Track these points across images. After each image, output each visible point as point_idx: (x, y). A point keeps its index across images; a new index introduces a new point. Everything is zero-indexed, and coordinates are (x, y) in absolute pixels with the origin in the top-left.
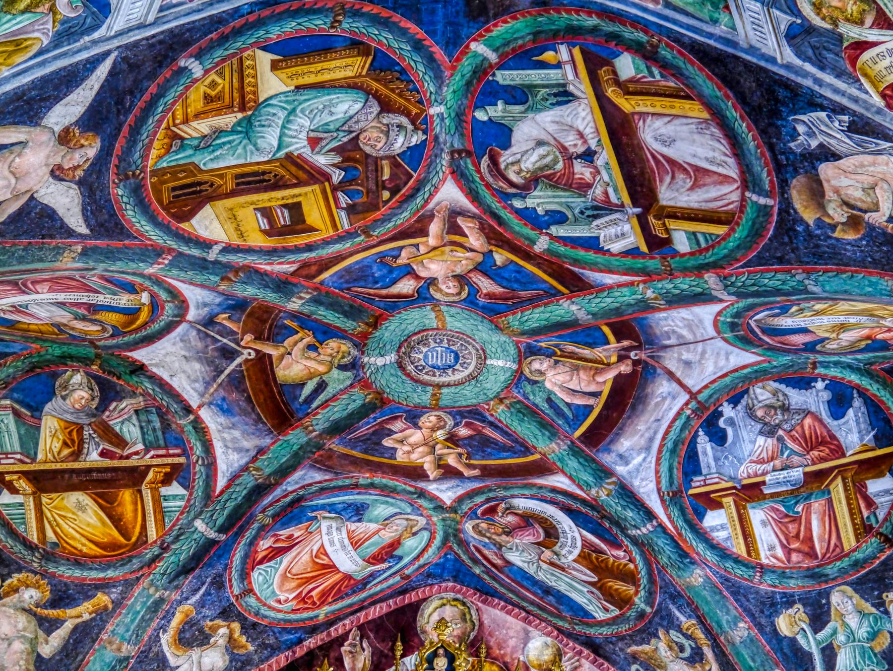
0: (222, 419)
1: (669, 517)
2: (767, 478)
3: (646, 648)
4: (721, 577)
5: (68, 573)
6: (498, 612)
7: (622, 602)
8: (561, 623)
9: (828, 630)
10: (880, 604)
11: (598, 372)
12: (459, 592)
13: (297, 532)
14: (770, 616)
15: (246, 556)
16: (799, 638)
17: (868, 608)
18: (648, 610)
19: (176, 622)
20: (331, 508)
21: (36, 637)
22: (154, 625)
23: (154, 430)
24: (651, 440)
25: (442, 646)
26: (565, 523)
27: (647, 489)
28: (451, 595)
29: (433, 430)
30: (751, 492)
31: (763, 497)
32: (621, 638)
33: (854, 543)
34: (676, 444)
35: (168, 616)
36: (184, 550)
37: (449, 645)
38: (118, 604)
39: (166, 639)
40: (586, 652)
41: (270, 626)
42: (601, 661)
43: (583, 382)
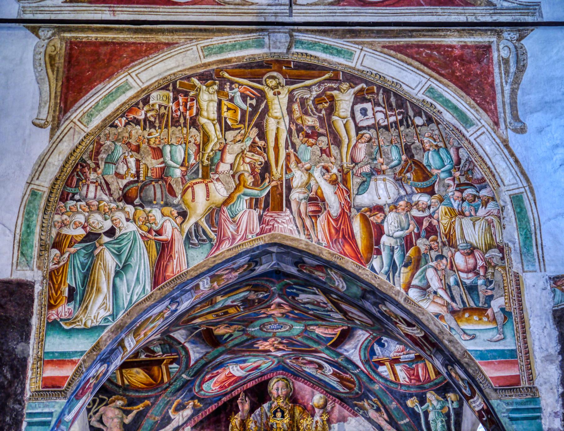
0: (193, 345)
1: (365, 368)
2: (401, 357)
3: (360, 403)
4: (385, 387)
5: (134, 394)
6: (301, 383)
7: (350, 389)
8: (327, 390)
9: (426, 406)
10: (445, 397)
11: (335, 329)
12: (284, 375)
13: (220, 371)
14: (404, 400)
15: (201, 381)
16: (415, 408)
17: (440, 398)
18: (360, 392)
19: (174, 406)
20: (234, 362)
21: (123, 417)
22: (167, 408)
23: (166, 348)
24: (357, 346)
25: (279, 408)
26: (326, 365)
27: (356, 359)
28: (281, 376)
29: (273, 341)
30: (396, 361)
31: (401, 362)
32: (350, 398)
33: (435, 377)
34: (366, 347)
35: (171, 405)
36: (178, 384)
37: (282, 407)
38: (153, 404)
39: (170, 411)
40: (337, 400)
41: (209, 398)
42: (343, 403)
43: (330, 331)
